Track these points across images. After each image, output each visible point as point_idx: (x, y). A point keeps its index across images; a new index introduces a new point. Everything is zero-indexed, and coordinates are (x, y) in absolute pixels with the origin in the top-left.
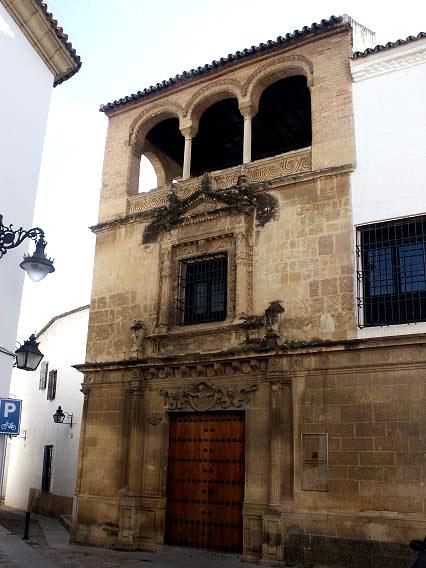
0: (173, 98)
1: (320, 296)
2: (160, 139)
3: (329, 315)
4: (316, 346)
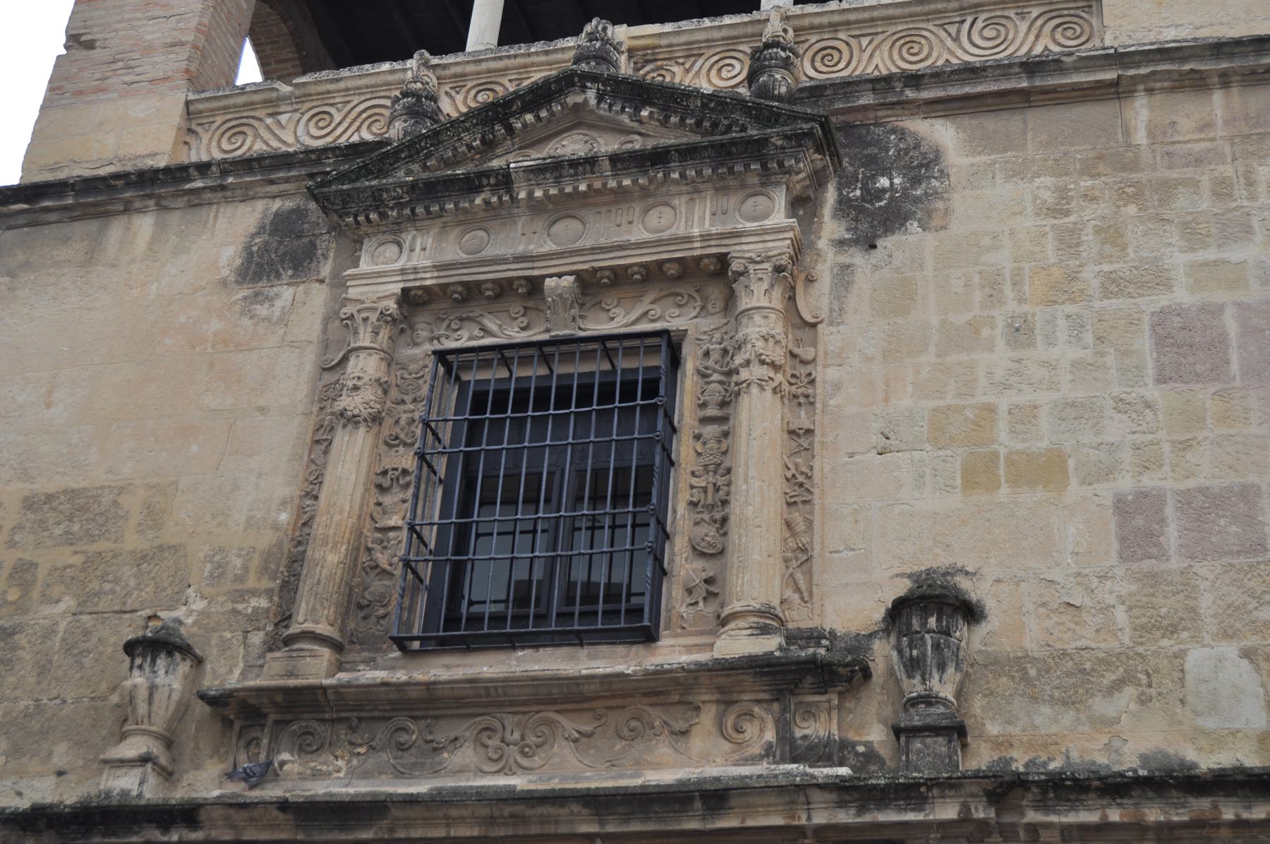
1: (1176, 563)
3: (1230, 650)
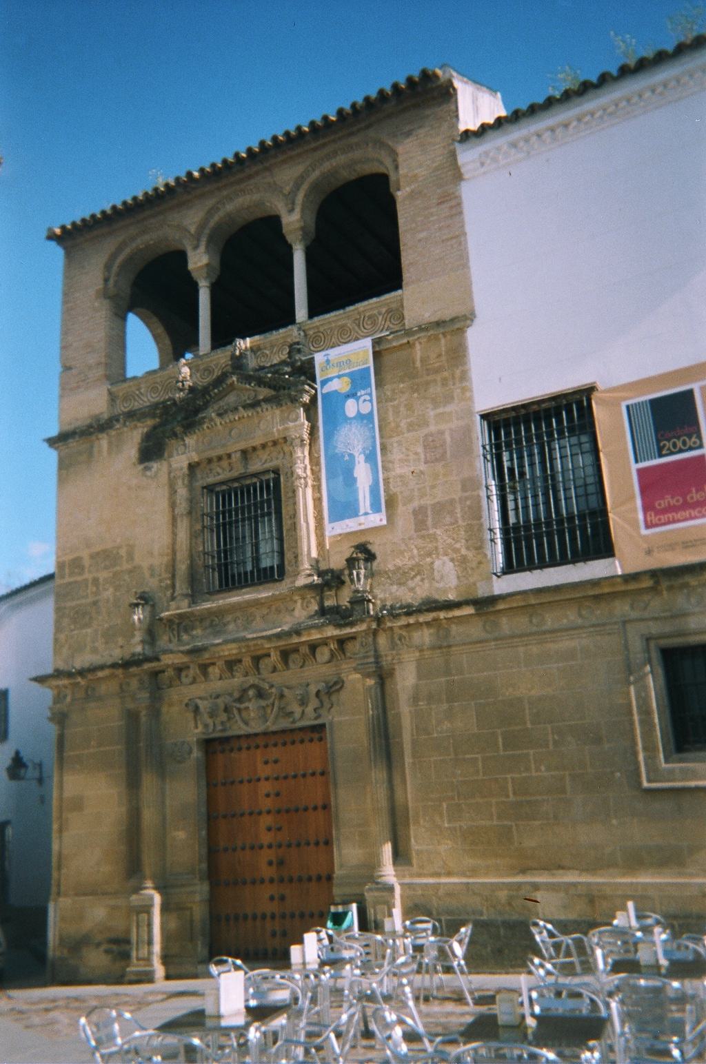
0: (174, 218)
2: (156, 289)
4: (429, 610)
